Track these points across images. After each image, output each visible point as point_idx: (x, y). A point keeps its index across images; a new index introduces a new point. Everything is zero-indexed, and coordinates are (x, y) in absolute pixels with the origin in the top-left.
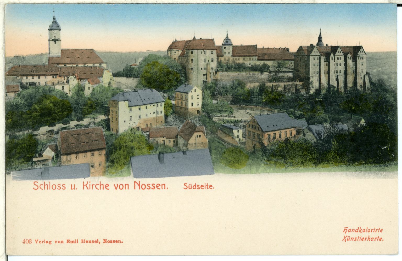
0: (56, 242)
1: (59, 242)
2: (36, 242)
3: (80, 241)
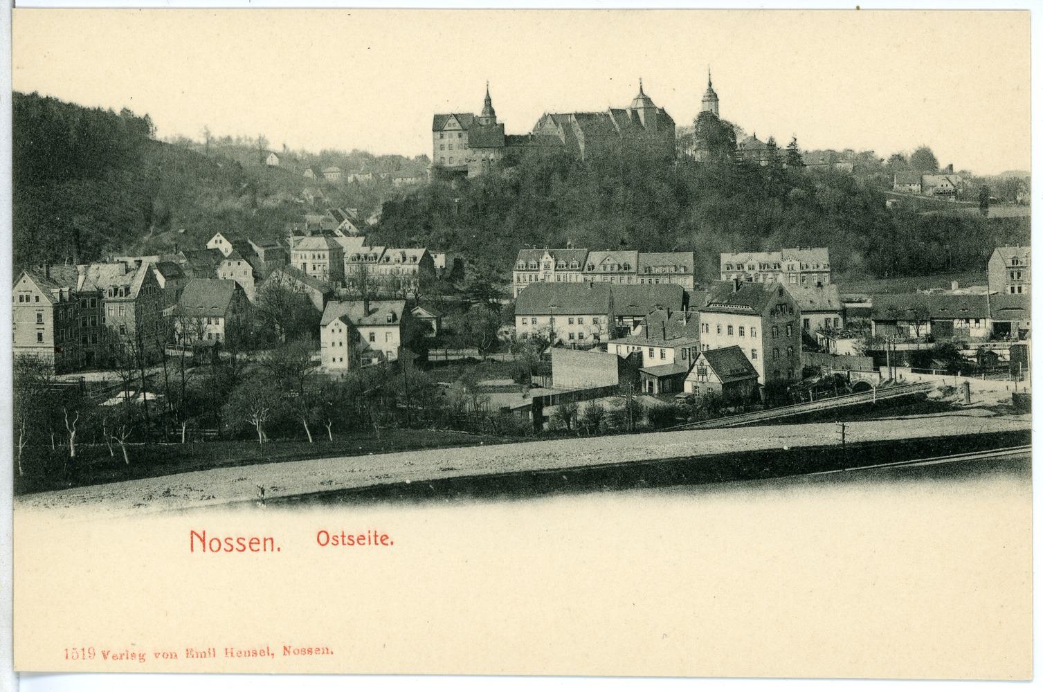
0: (156, 655)
1: (165, 655)
2: (105, 657)
3: (220, 652)
